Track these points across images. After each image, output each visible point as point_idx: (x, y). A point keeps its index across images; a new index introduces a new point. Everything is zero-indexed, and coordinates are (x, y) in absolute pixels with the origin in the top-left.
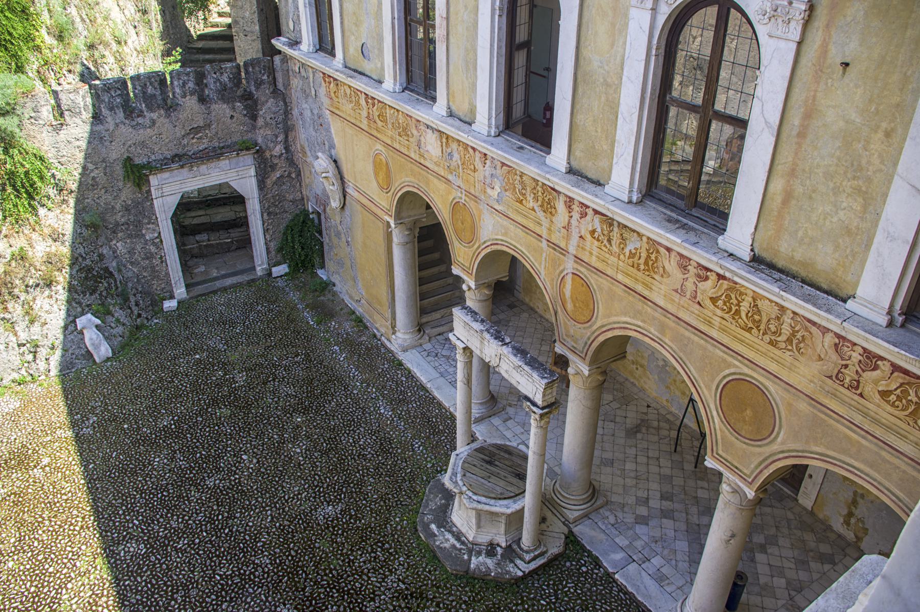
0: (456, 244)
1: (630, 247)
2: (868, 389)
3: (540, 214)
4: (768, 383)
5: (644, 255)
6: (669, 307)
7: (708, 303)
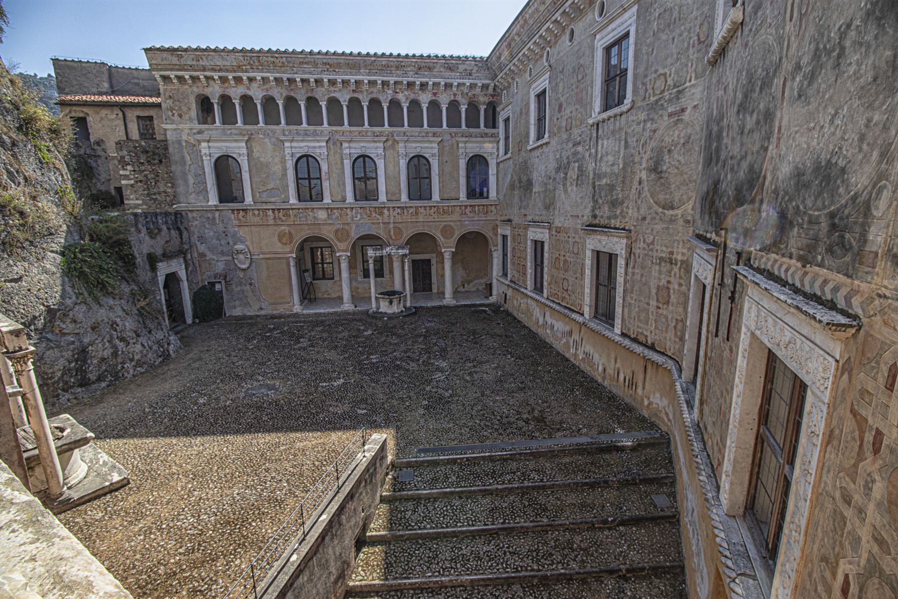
0: (338, 244)
1: (410, 212)
2: (468, 213)
3: (378, 216)
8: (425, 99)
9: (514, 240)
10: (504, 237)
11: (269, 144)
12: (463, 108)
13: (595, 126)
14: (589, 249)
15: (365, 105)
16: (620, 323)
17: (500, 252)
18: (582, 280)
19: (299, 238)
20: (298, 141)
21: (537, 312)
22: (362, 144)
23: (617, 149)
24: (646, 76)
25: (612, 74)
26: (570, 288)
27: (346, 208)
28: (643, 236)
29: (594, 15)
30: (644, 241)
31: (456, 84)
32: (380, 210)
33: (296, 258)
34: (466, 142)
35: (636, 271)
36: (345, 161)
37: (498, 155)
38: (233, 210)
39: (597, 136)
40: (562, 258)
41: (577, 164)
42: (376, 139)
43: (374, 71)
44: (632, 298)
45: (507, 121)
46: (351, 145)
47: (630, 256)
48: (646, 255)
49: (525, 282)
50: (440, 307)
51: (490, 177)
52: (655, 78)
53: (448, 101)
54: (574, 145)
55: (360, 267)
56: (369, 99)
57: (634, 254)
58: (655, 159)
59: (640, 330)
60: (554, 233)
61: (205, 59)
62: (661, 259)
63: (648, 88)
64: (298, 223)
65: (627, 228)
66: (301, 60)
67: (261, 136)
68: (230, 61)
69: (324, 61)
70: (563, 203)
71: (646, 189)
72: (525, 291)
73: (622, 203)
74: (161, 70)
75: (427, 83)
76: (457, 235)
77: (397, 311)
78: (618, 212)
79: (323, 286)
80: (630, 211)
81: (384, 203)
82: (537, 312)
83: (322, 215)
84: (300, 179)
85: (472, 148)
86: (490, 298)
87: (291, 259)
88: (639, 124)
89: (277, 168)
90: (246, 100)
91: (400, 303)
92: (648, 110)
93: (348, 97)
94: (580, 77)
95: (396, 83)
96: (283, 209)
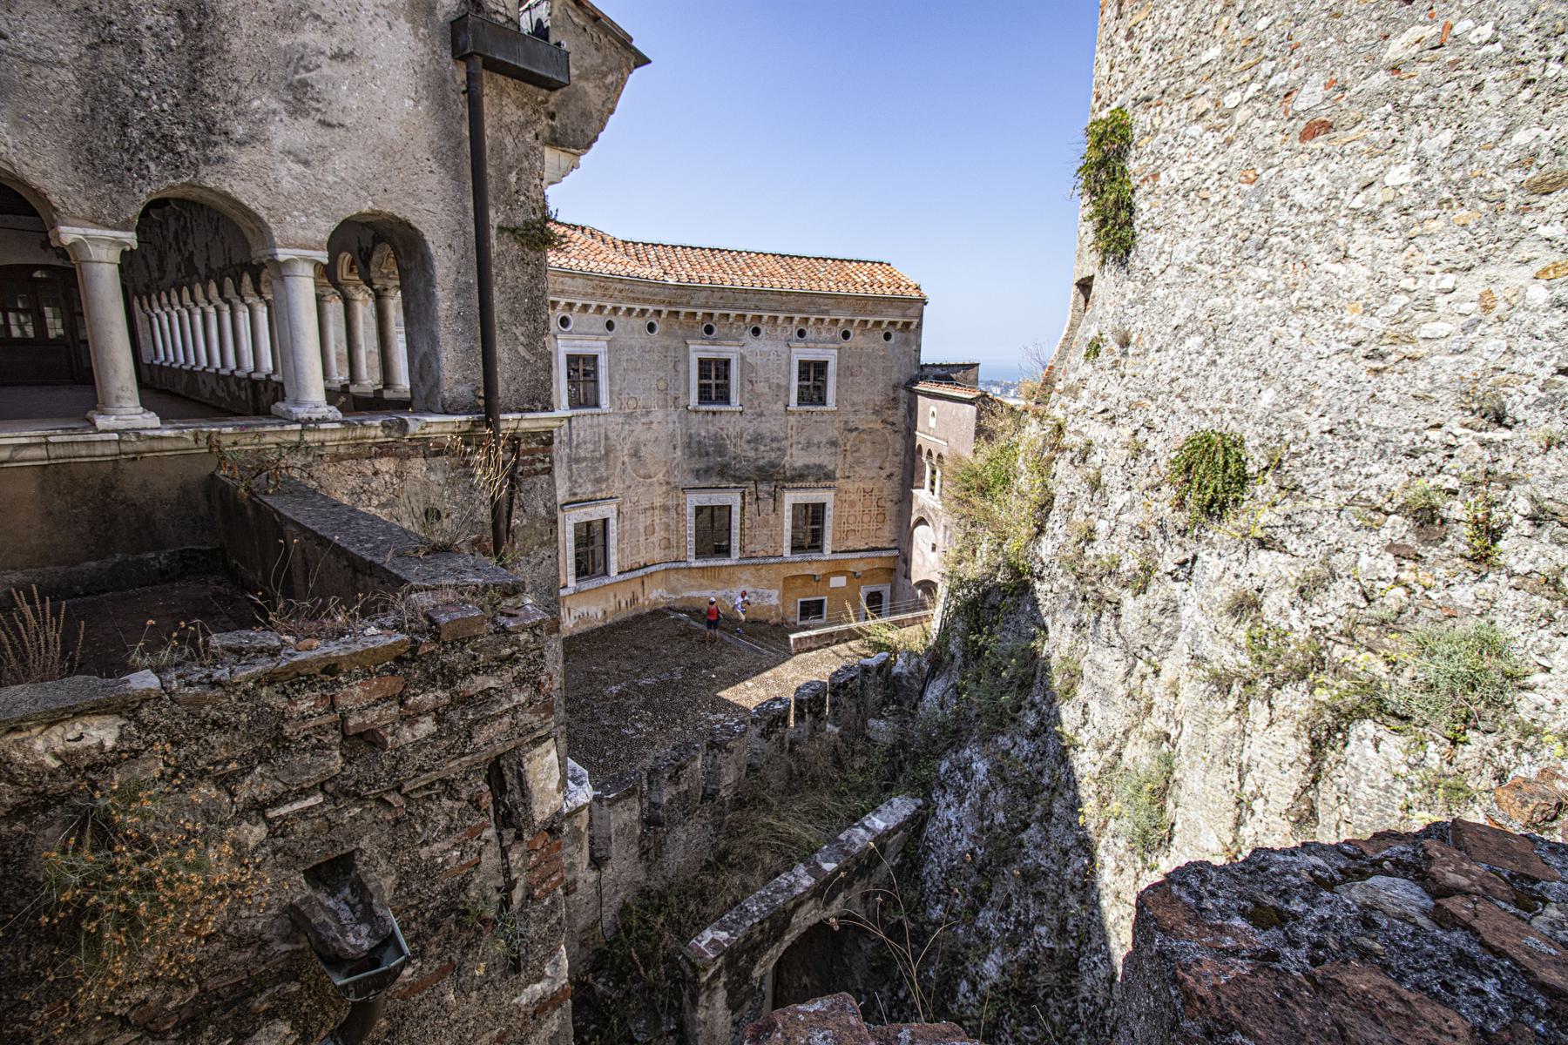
62: (646, 509)
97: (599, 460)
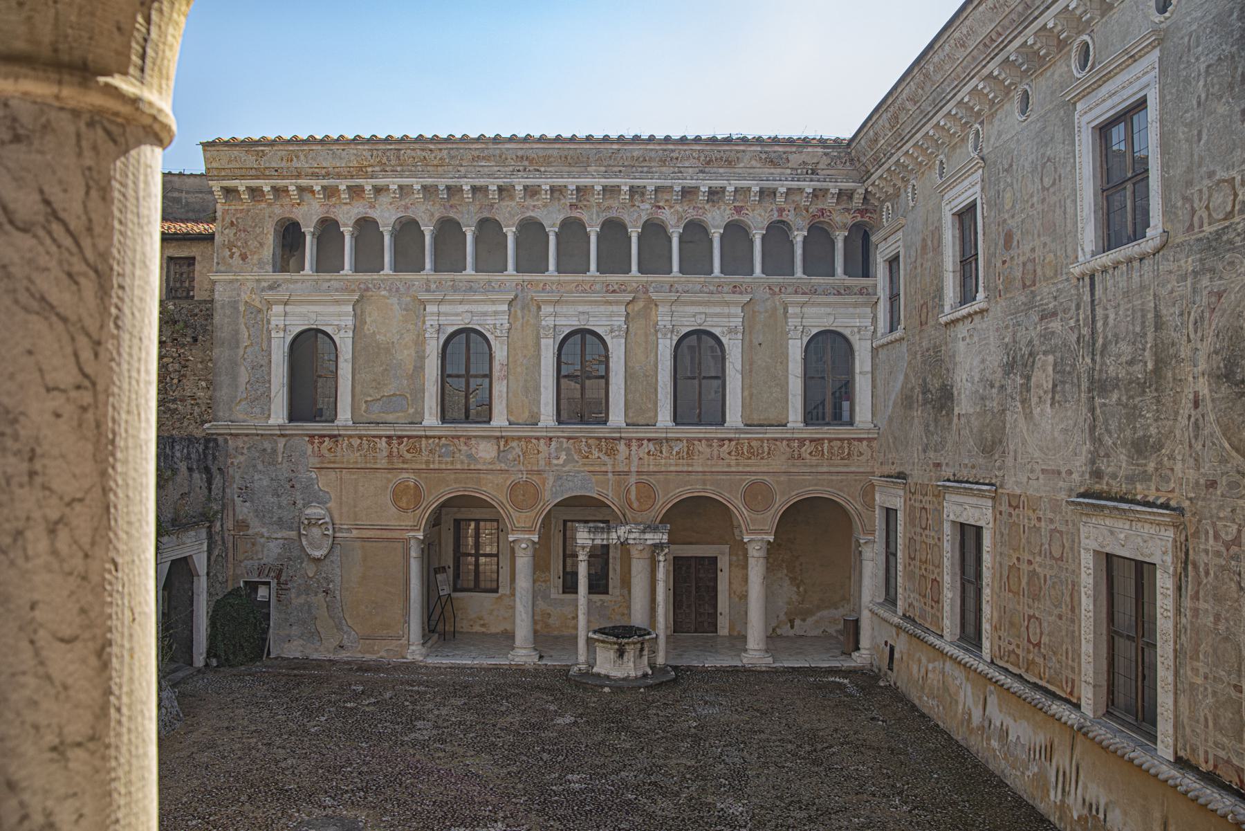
0: (514, 514)
1: (676, 449)
2: (804, 455)
4: (765, 478)
5: (685, 450)
6: (706, 469)
7: (727, 456)
8: (716, 220)
9: (911, 520)
10: (890, 513)
11: (396, 307)
12: (799, 237)
13: (1087, 280)
14: (1087, 550)
15: (593, 232)
16: (1171, 731)
17: (880, 547)
18: (1073, 621)
19: (432, 501)
20: (452, 302)
21: (967, 696)
22: (581, 309)
23: (1138, 329)
24: (1189, 184)
25: (1116, 179)
26: (1045, 639)
27: (538, 438)
28: (1214, 525)
29: (1069, 66)
30: (1217, 537)
31: (783, 190)
32: (610, 445)
33: (423, 541)
34: (803, 305)
35: (1202, 605)
36: (543, 341)
37: (875, 331)
38: (312, 436)
39: (1093, 301)
40: (1024, 567)
41: (1051, 358)
42: (611, 297)
43: (616, 169)
44: (1196, 671)
45: (893, 262)
46: (558, 309)
47: (1185, 569)
48: (1223, 568)
49: (938, 620)
50: (735, 671)
51: (857, 377)
52: (1210, 188)
53: (766, 223)
54: (1042, 319)
55: (557, 567)
56: (601, 220)
57: (1195, 566)
58: (1225, 354)
59: (1222, 754)
60: (1004, 508)
61: (302, 157)
63: (1195, 205)
64: (436, 466)
65: (1173, 503)
66: (477, 153)
67: (383, 293)
68: (349, 158)
69: (520, 153)
70: (1024, 443)
71: (1212, 417)
72: (937, 642)
73: (1158, 447)
74: (224, 178)
75: (723, 189)
76: (781, 503)
77: (633, 674)
78: (1151, 466)
79: (475, 605)
80: (1179, 467)
81: (619, 430)
82: (967, 696)
83: (486, 451)
84: (449, 376)
85: (819, 317)
86: (855, 655)
87: (413, 542)
88: (1183, 278)
89: (406, 355)
90: (366, 226)
91: (641, 656)
92: (1201, 251)
93: (561, 217)
94: (1047, 181)
95: (658, 190)
96: (409, 437)
97: (1143, 387)
